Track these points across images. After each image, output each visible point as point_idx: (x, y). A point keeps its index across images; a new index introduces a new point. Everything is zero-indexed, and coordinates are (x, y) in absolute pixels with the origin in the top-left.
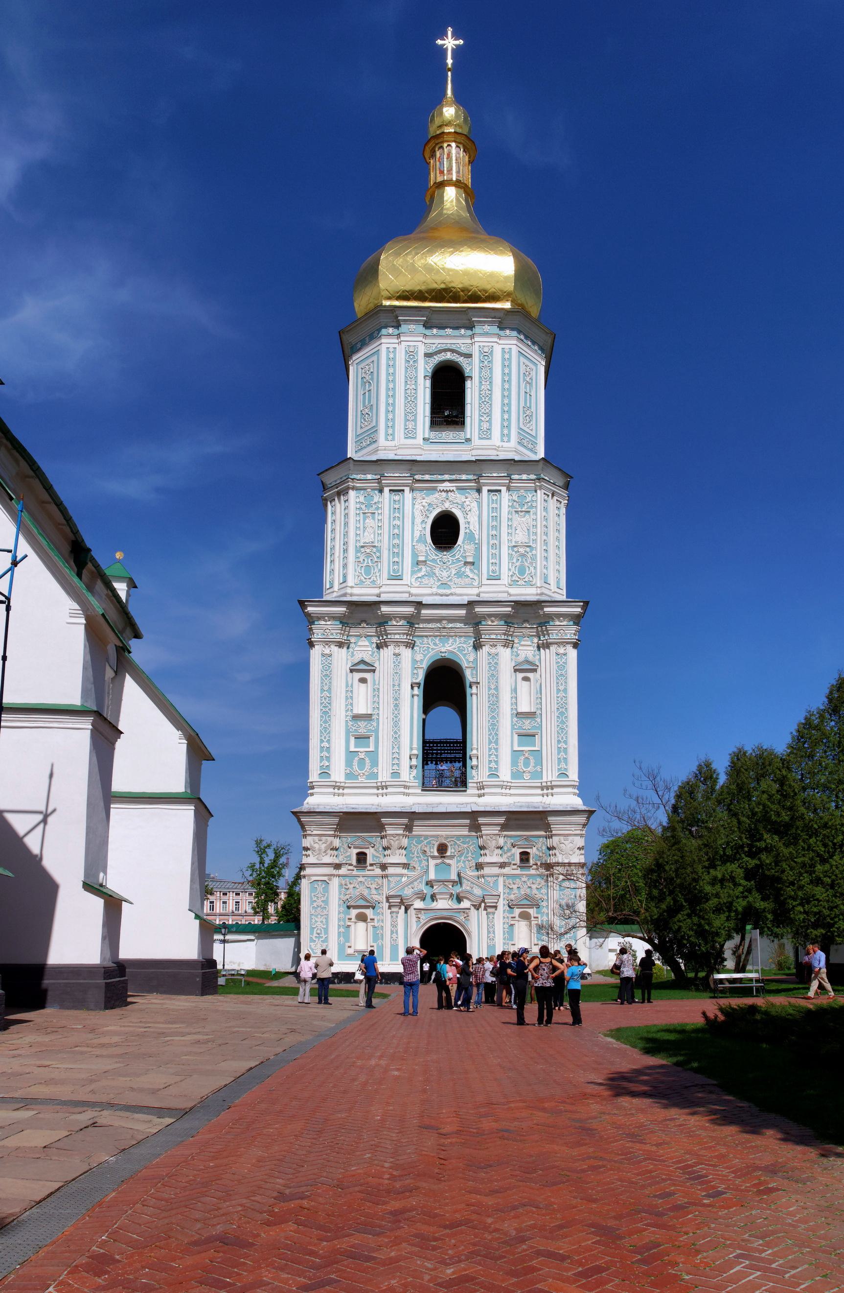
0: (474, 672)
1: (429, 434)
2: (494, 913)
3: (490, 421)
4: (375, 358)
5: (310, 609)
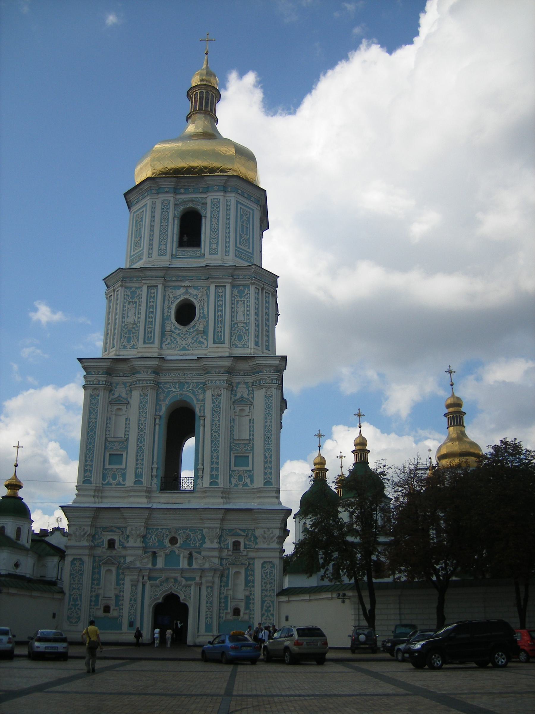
0: (202, 408)
1: (177, 251)
2: (212, 588)
3: (217, 243)
4: (144, 209)
5: (85, 364)
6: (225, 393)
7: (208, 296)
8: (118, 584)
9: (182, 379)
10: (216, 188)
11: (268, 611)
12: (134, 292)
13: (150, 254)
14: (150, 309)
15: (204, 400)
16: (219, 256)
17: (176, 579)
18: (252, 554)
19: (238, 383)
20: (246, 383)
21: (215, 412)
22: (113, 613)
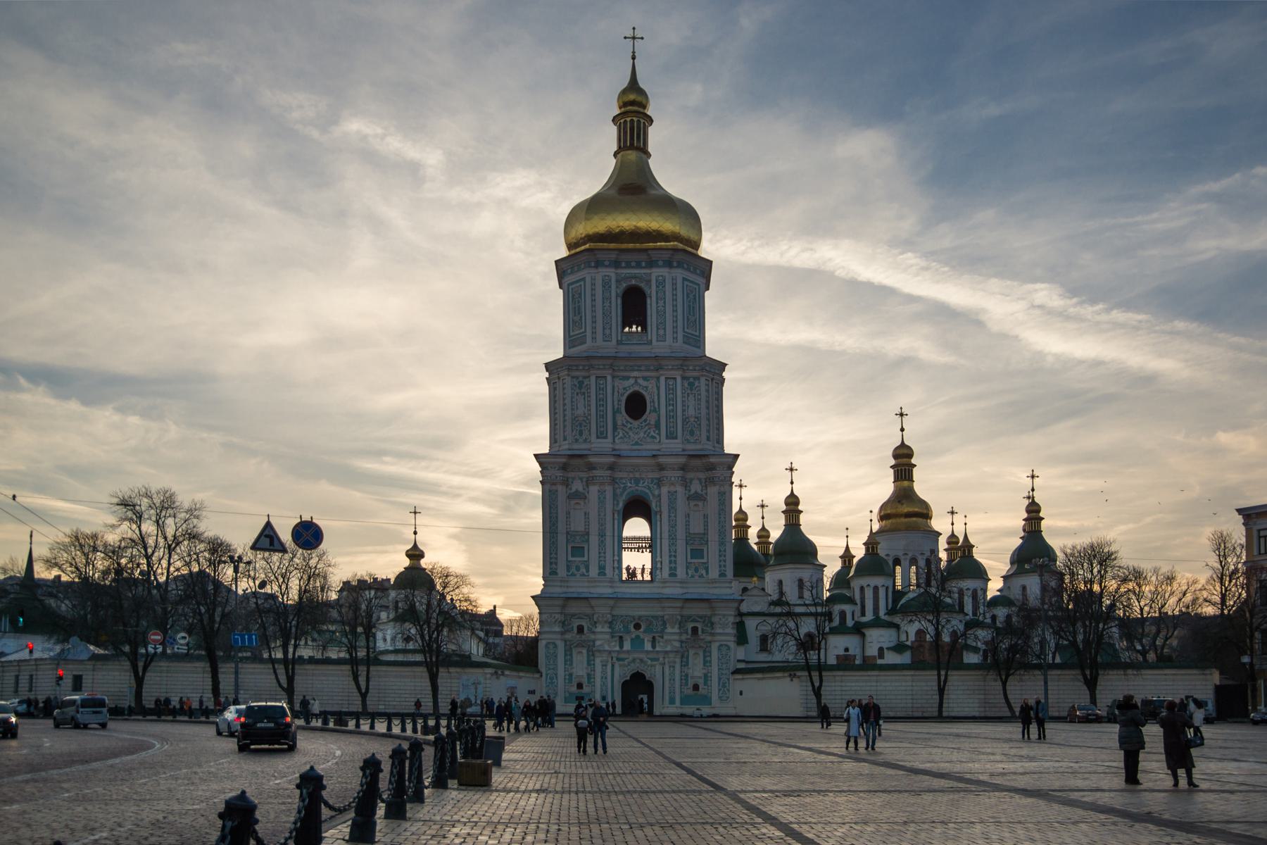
6: (680, 489)
7: (658, 388)
8: (589, 664)
9: (637, 475)
10: (661, 263)
11: (724, 686)
12: (581, 383)
13: (594, 339)
14: (601, 402)
15: (659, 495)
16: (667, 343)
17: (642, 660)
18: (709, 638)
19: (691, 480)
20: (700, 480)
21: (672, 508)
22: (586, 689)
